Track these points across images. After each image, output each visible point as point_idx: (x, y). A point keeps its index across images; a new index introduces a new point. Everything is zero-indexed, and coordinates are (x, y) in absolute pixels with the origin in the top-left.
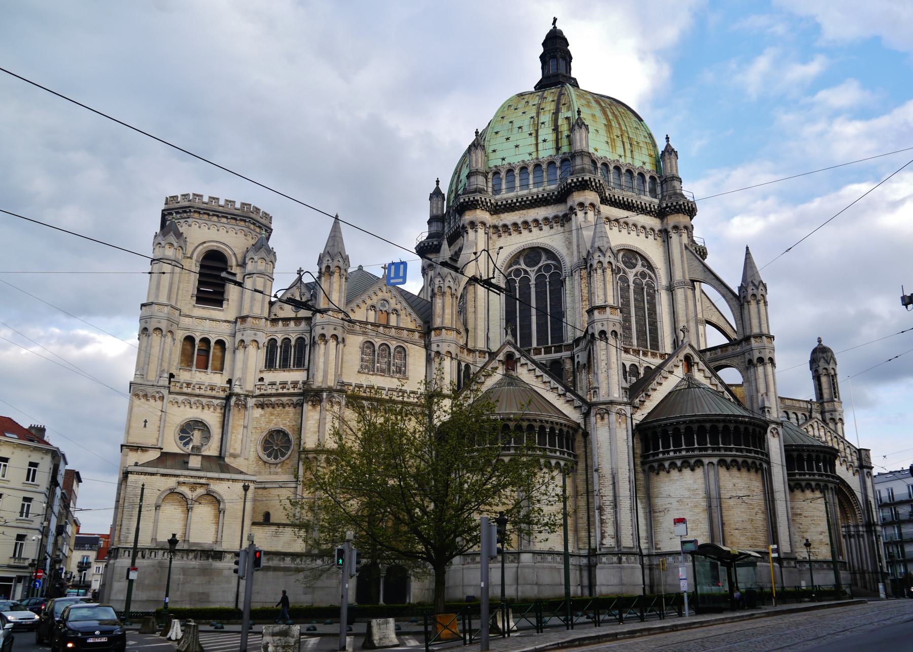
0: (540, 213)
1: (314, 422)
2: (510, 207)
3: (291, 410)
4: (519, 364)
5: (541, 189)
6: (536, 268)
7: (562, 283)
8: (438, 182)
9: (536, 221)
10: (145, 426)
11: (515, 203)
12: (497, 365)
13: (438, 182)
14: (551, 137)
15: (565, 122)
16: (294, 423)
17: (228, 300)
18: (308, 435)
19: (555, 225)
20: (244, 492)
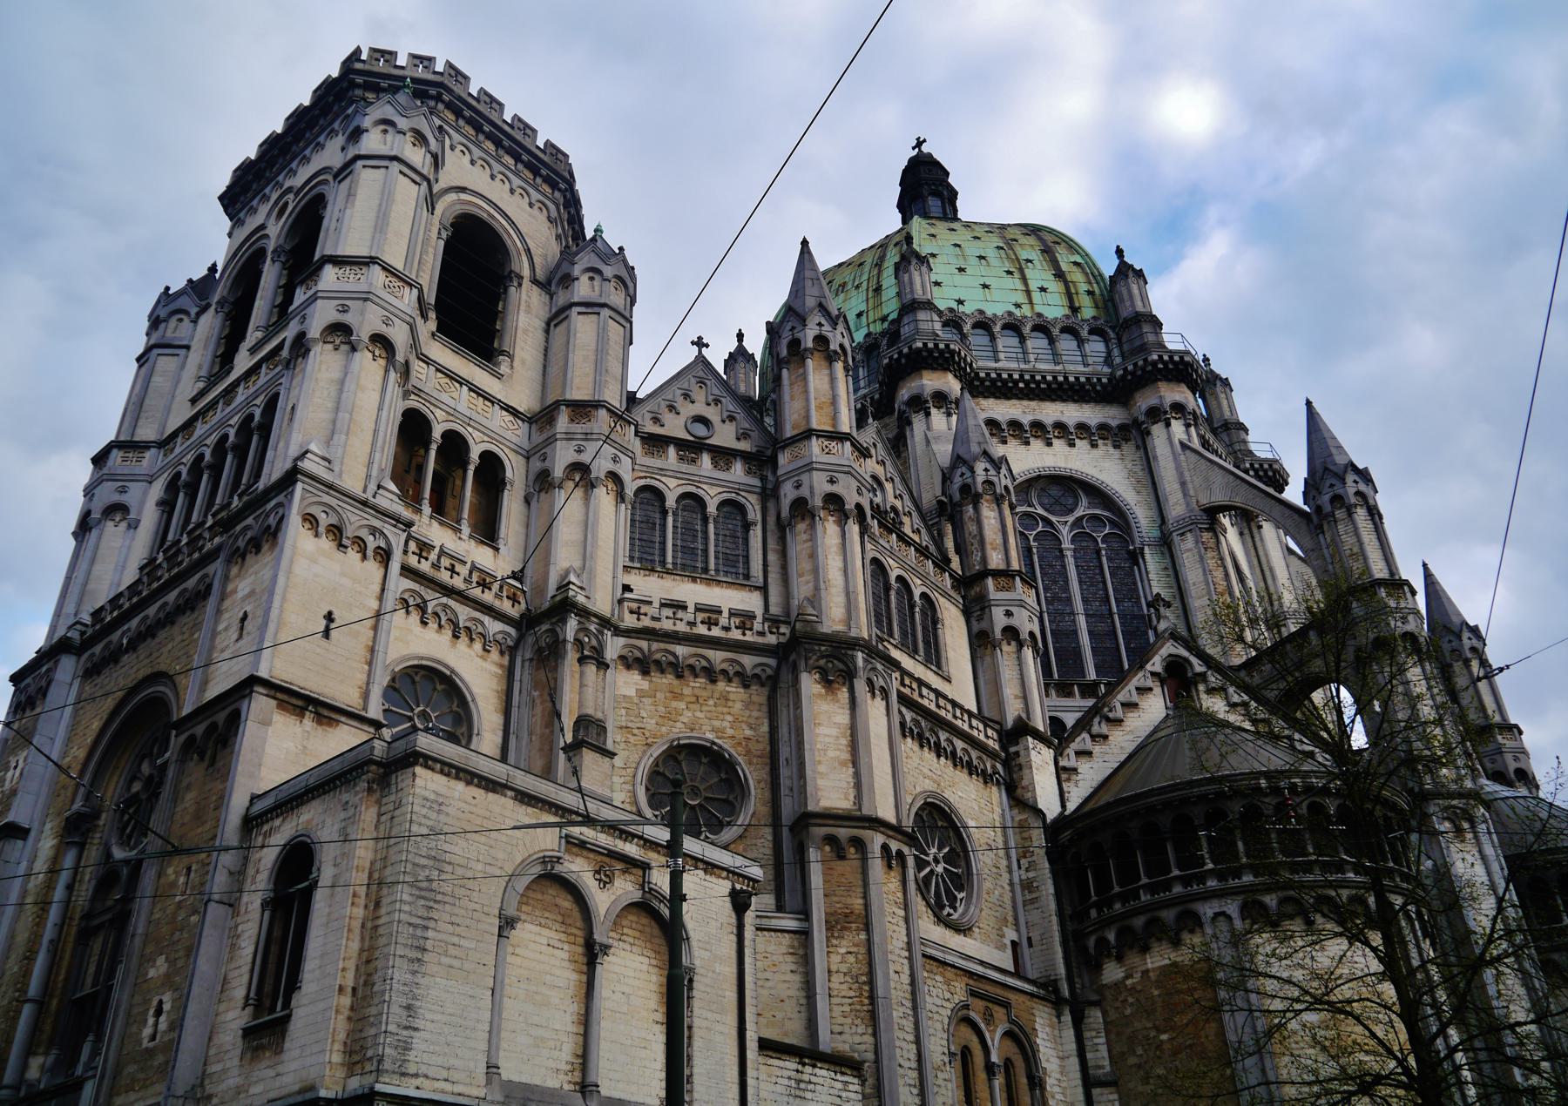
0: (1071, 413)
1: (834, 732)
2: (1003, 388)
3: (734, 690)
4: (1201, 687)
5: (1058, 368)
6: (1071, 519)
7: (1135, 557)
8: (740, 336)
9: (1060, 426)
10: (326, 633)
11: (1016, 382)
12: (1149, 683)
13: (740, 336)
14: (1055, 286)
15: (1075, 269)
16: (748, 732)
17: (511, 357)
18: (822, 768)
19: (1100, 442)
20: (734, 921)
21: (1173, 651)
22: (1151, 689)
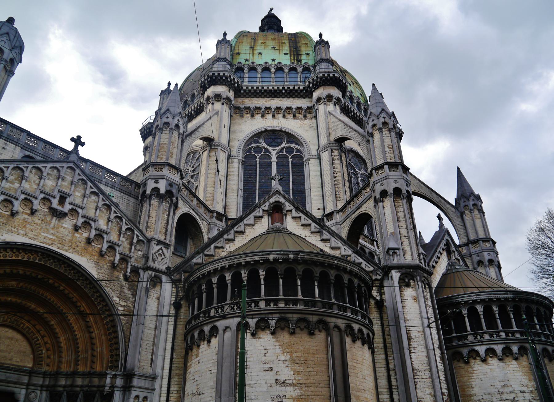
21: (277, 199)
22: (262, 217)
